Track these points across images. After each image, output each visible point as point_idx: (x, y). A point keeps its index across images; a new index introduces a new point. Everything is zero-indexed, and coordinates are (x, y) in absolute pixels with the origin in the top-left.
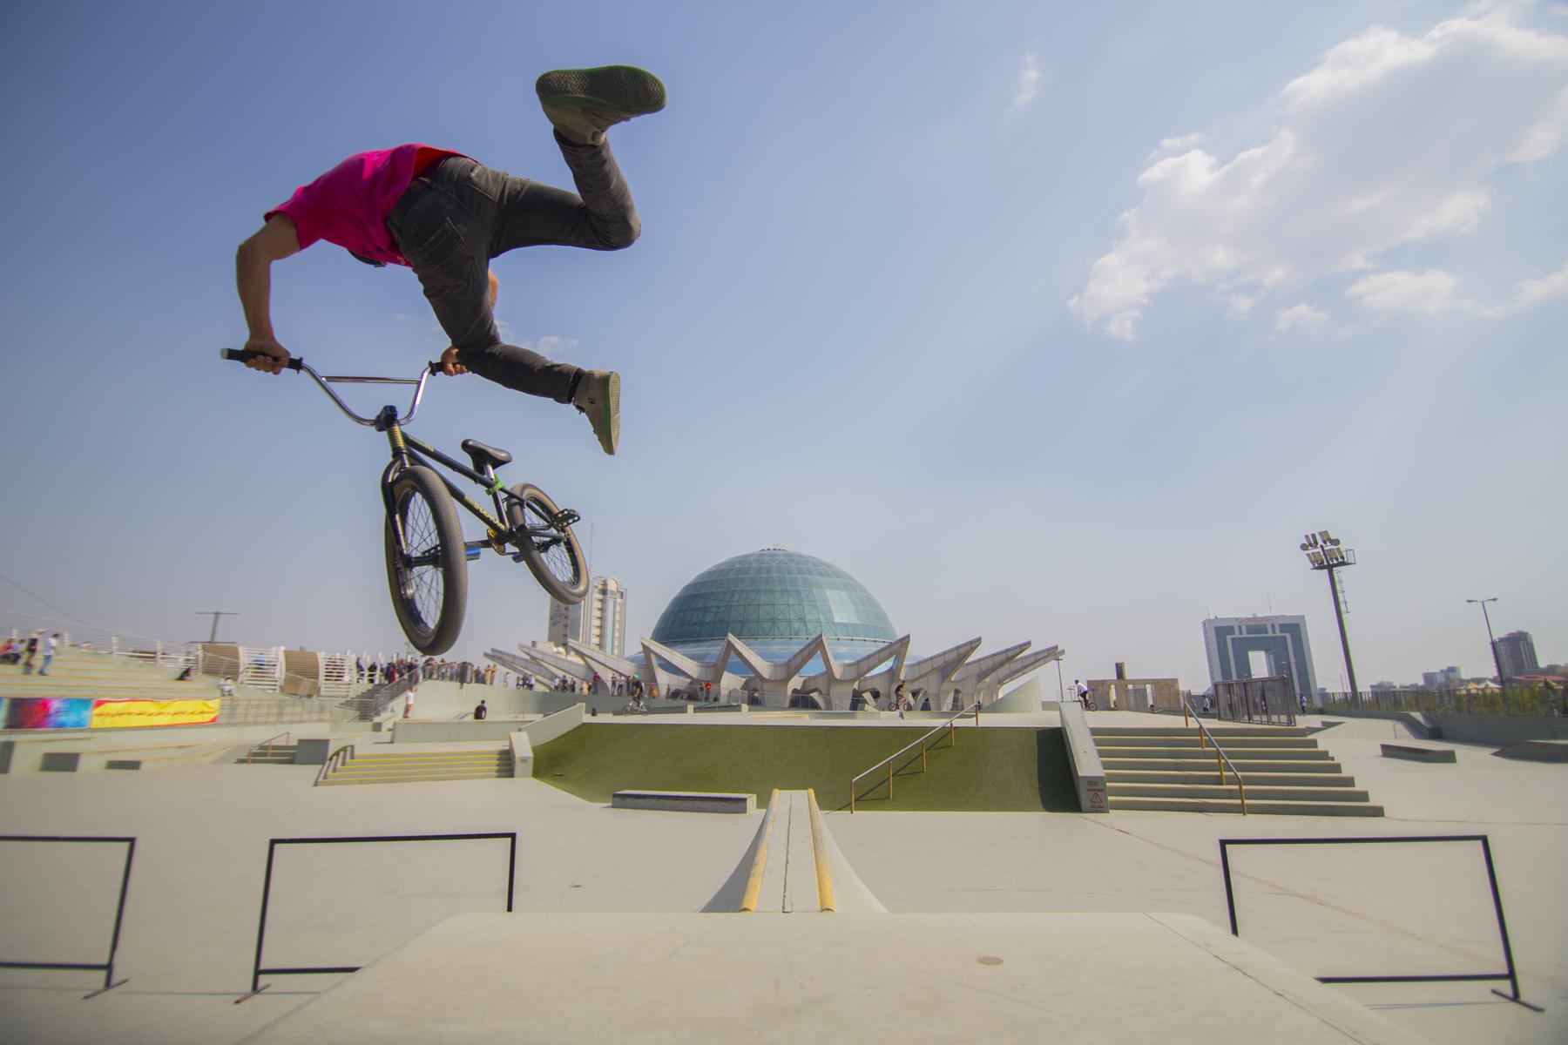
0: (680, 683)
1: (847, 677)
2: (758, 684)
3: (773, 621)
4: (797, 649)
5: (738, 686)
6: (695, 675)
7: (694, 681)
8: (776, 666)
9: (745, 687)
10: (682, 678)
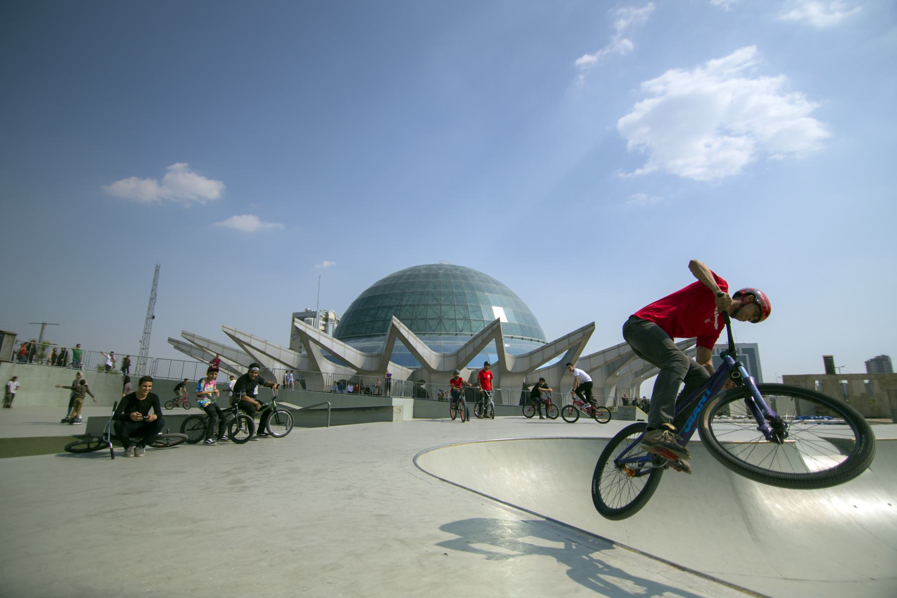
0: (347, 373)
1: (518, 370)
2: (425, 375)
3: (440, 319)
4: (462, 343)
5: (404, 379)
6: (359, 365)
7: (360, 371)
8: (444, 356)
9: (412, 377)
10: (349, 369)
